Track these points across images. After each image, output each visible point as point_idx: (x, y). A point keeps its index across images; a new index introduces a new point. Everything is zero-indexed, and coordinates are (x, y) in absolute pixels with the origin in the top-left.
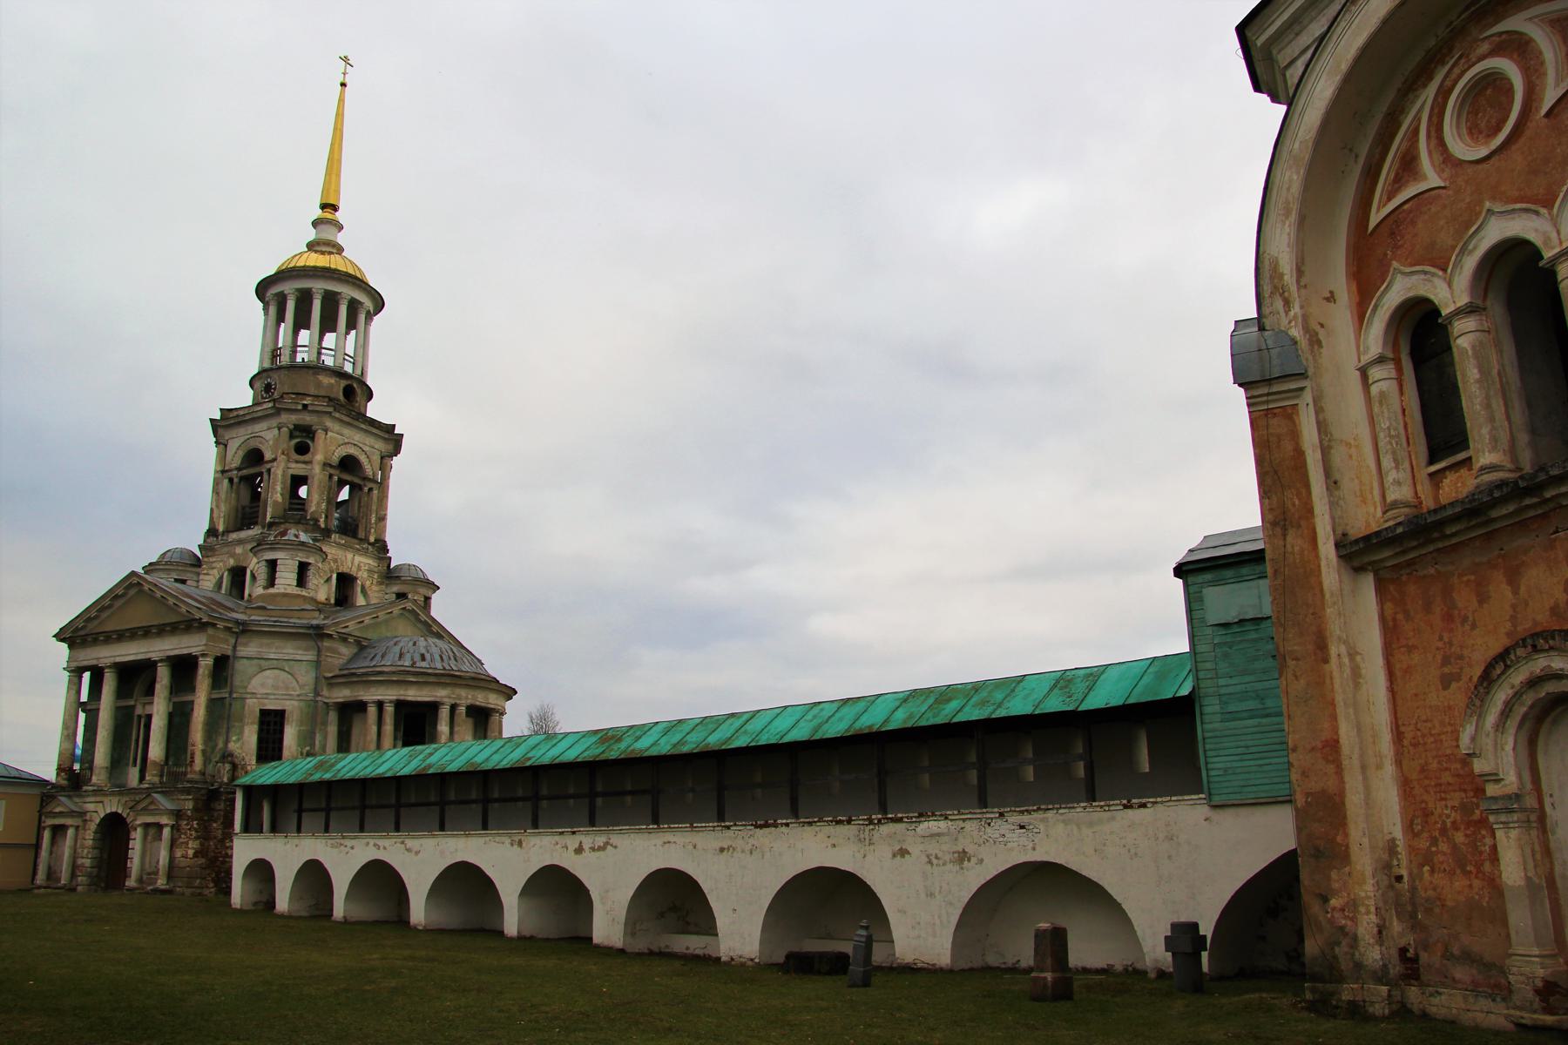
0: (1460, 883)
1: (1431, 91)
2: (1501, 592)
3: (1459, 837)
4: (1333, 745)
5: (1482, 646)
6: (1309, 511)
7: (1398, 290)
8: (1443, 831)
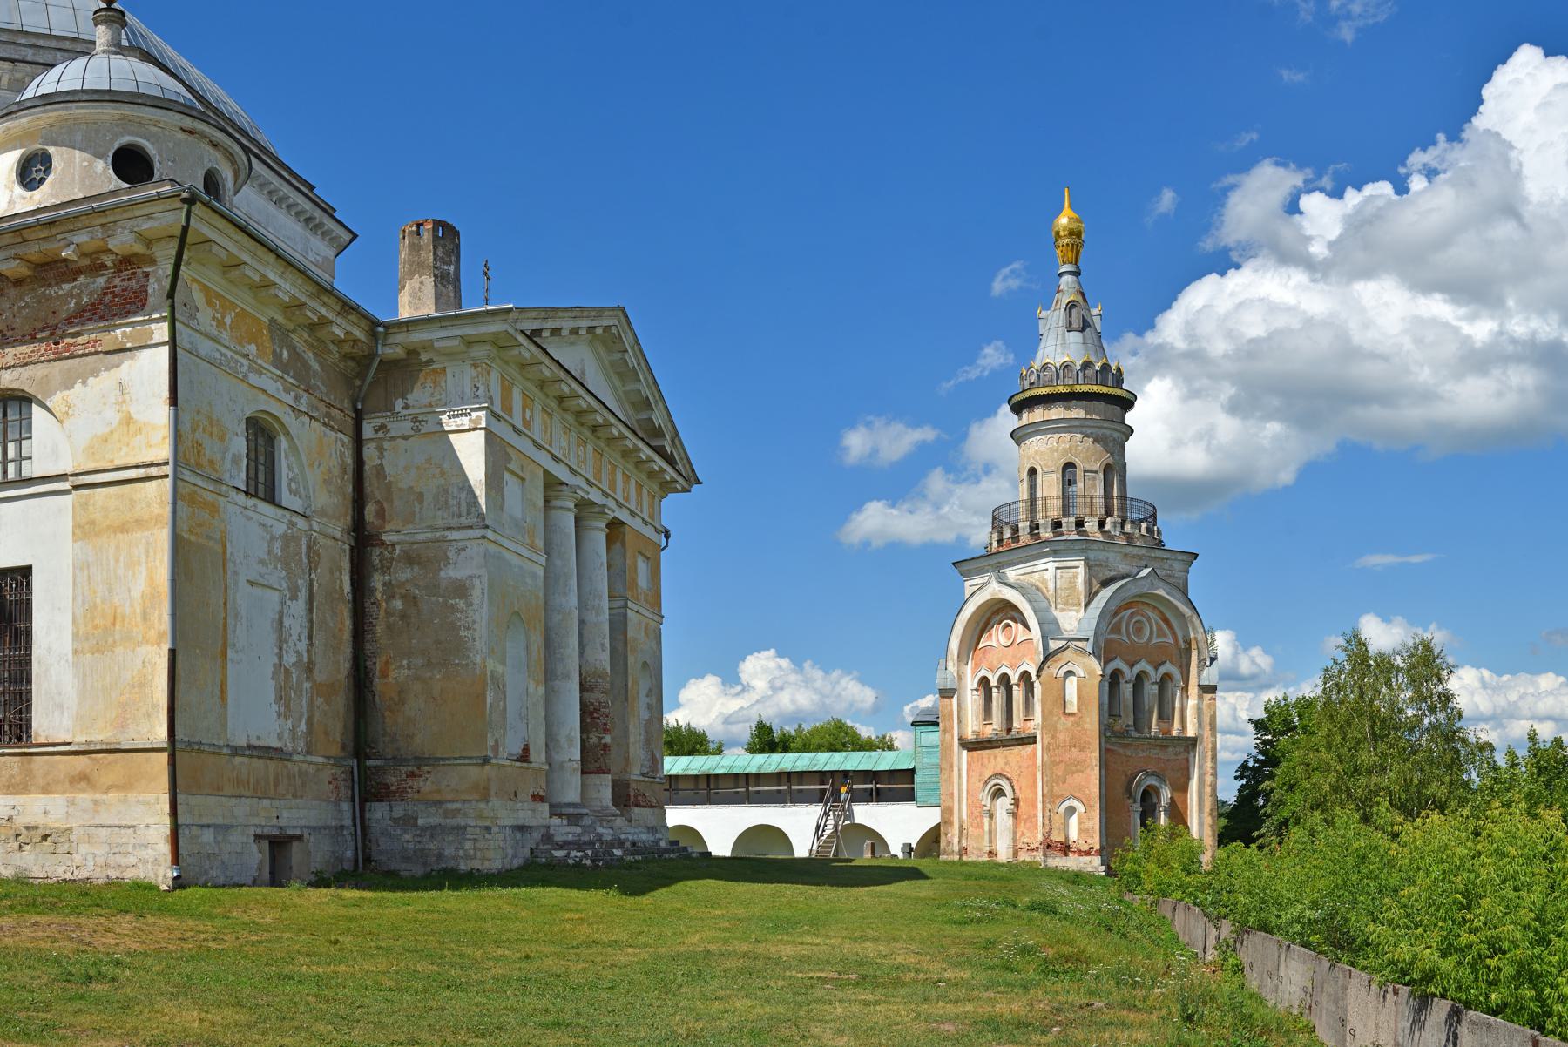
4: (952, 794)
7: (983, 673)
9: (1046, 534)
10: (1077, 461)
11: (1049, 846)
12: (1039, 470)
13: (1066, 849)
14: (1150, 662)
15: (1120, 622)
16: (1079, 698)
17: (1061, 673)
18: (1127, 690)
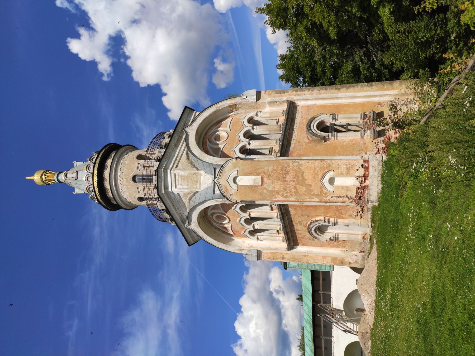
1: (214, 223)
2: (299, 232)
5: (308, 235)
7: (247, 233)
10: (132, 175)
11: (360, 198)
16: (251, 174)
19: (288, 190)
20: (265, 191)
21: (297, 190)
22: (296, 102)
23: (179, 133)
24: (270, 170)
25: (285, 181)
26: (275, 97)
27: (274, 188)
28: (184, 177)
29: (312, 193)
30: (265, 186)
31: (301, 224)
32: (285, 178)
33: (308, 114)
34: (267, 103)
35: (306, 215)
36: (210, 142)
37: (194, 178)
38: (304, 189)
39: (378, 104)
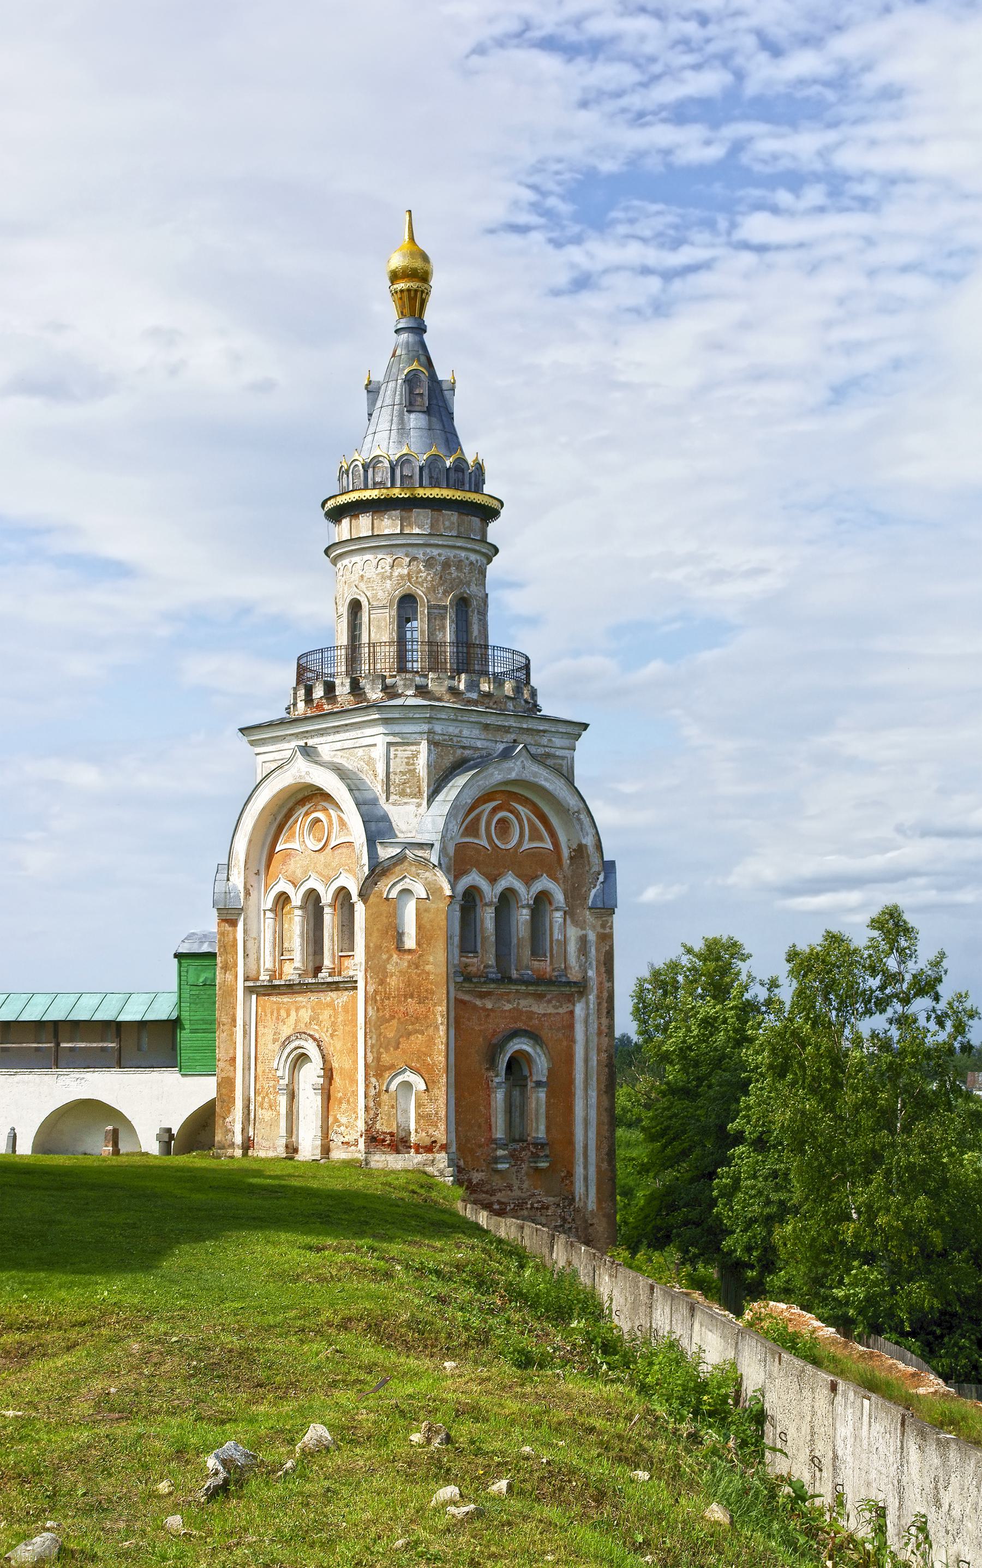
0: (270, 1112)
3: (271, 1097)
5: (286, 1031)
6: (236, 965)
8: (267, 1094)
9: (375, 694)
12: (365, 603)
13: (399, 1144)
14: (519, 876)
15: (478, 819)
16: (419, 927)
17: (393, 894)
18: (488, 918)
19: (387, 1002)
20: (385, 957)
21: (388, 1021)
22: (584, 1000)
23: (518, 725)
24: (428, 968)
25: (405, 997)
26: (597, 950)
27: (392, 976)
28: (413, 764)
29: (382, 1050)
30: (395, 956)
31: (312, 1019)
32: (412, 997)
33: (551, 1029)
34: (584, 932)
35: (335, 1031)
36: (495, 810)
37: (410, 787)
38: (391, 1035)
39: (568, 1172)
